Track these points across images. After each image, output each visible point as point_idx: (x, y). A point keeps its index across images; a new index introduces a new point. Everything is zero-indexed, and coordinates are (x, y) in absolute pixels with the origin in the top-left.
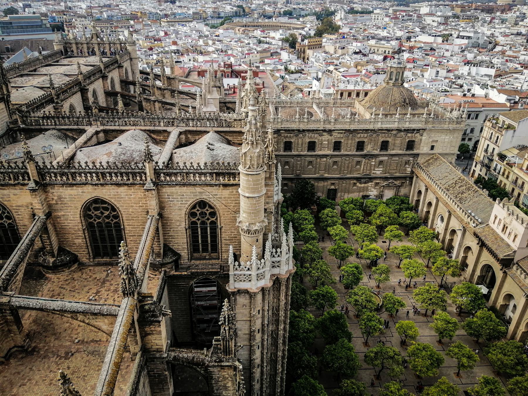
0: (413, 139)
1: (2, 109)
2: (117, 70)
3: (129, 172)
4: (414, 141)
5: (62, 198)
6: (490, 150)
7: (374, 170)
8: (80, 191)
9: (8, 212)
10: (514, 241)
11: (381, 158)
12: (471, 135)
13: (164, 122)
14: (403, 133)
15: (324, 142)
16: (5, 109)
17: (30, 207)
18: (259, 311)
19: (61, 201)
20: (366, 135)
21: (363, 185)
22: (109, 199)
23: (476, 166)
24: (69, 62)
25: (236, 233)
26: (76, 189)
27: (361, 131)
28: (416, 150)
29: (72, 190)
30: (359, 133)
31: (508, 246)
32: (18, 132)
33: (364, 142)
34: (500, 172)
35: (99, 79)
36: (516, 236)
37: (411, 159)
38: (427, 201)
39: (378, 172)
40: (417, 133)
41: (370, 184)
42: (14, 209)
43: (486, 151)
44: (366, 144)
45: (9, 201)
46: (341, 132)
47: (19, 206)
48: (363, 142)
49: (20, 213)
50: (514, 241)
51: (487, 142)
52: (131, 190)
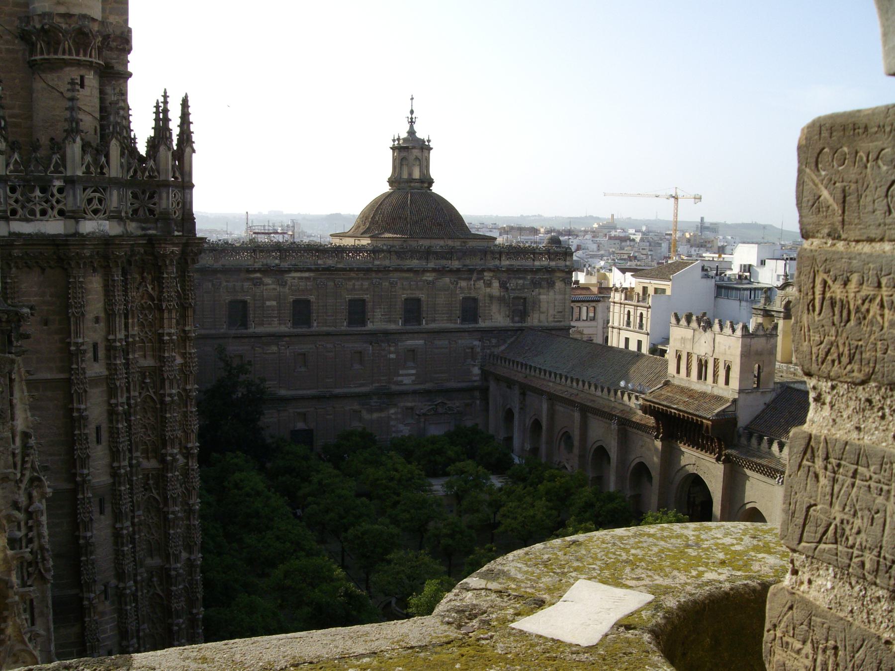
0: (473, 294)
4: (475, 300)
7: (399, 375)
11: (409, 342)
15: (268, 303)
18: (95, 346)
20: (366, 284)
21: (375, 416)
25: (16, 111)
27: (353, 275)
28: (484, 321)
30: (350, 279)
33: (364, 301)
37: (476, 343)
38: (529, 422)
39: (407, 380)
40: (479, 279)
41: (392, 411)
44: (369, 305)
46: (306, 275)
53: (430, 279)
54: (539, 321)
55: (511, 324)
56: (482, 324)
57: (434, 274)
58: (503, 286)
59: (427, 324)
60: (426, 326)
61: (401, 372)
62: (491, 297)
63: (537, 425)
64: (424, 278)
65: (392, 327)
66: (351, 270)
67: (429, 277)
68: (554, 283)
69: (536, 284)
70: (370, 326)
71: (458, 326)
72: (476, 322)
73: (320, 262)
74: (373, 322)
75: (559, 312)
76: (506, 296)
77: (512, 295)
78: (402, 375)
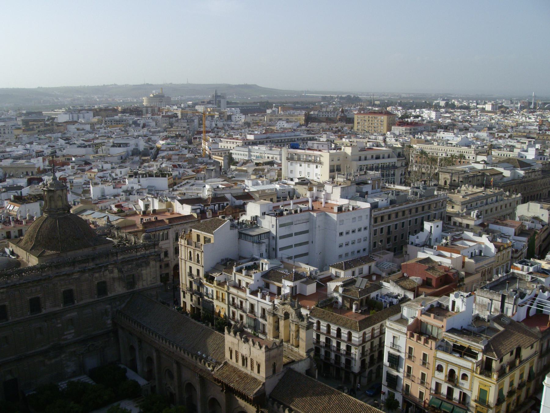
0: (103, 279)
4: (104, 282)
6: (194, 272)
10: (259, 372)
12: (166, 259)
14: (87, 275)
20: (39, 288)
21: (53, 361)
23: (184, 297)
27: (30, 284)
31: (255, 380)
34: (213, 296)
36: (259, 366)
37: (108, 306)
39: (69, 337)
40: (106, 270)
41: (63, 356)
43: (191, 274)
48: (38, 299)
50: (259, 372)
51: (189, 264)
53: (77, 276)
54: (143, 285)
55: (127, 291)
56: (110, 295)
57: (79, 274)
58: (120, 271)
59: (78, 302)
60: (77, 304)
61: (65, 333)
62: (114, 279)
63: (150, 360)
64: (73, 277)
65: (58, 309)
66: (29, 282)
67: (76, 276)
68: (149, 263)
69: (139, 266)
70: (44, 311)
71: (96, 299)
72: (107, 295)
73: (9, 281)
74: (45, 309)
75: (153, 278)
76: (123, 276)
77: (126, 275)
78: (67, 335)
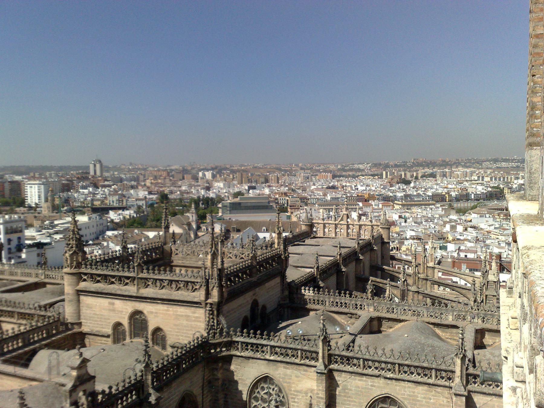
1: (278, 283)
2: (369, 253)
3: (432, 369)
5: (347, 389)
8: (370, 384)
9: (283, 397)
13: (453, 315)
16: (279, 284)
17: (309, 395)
19: (345, 392)
22: (401, 399)
24: (316, 242)
26: (365, 381)
29: (360, 380)
32: (286, 310)
35: (353, 261)
42: (291, 394)
45: (289, 383)
47: (297, 391)
49: (296, 400)
52: (432, 392)
